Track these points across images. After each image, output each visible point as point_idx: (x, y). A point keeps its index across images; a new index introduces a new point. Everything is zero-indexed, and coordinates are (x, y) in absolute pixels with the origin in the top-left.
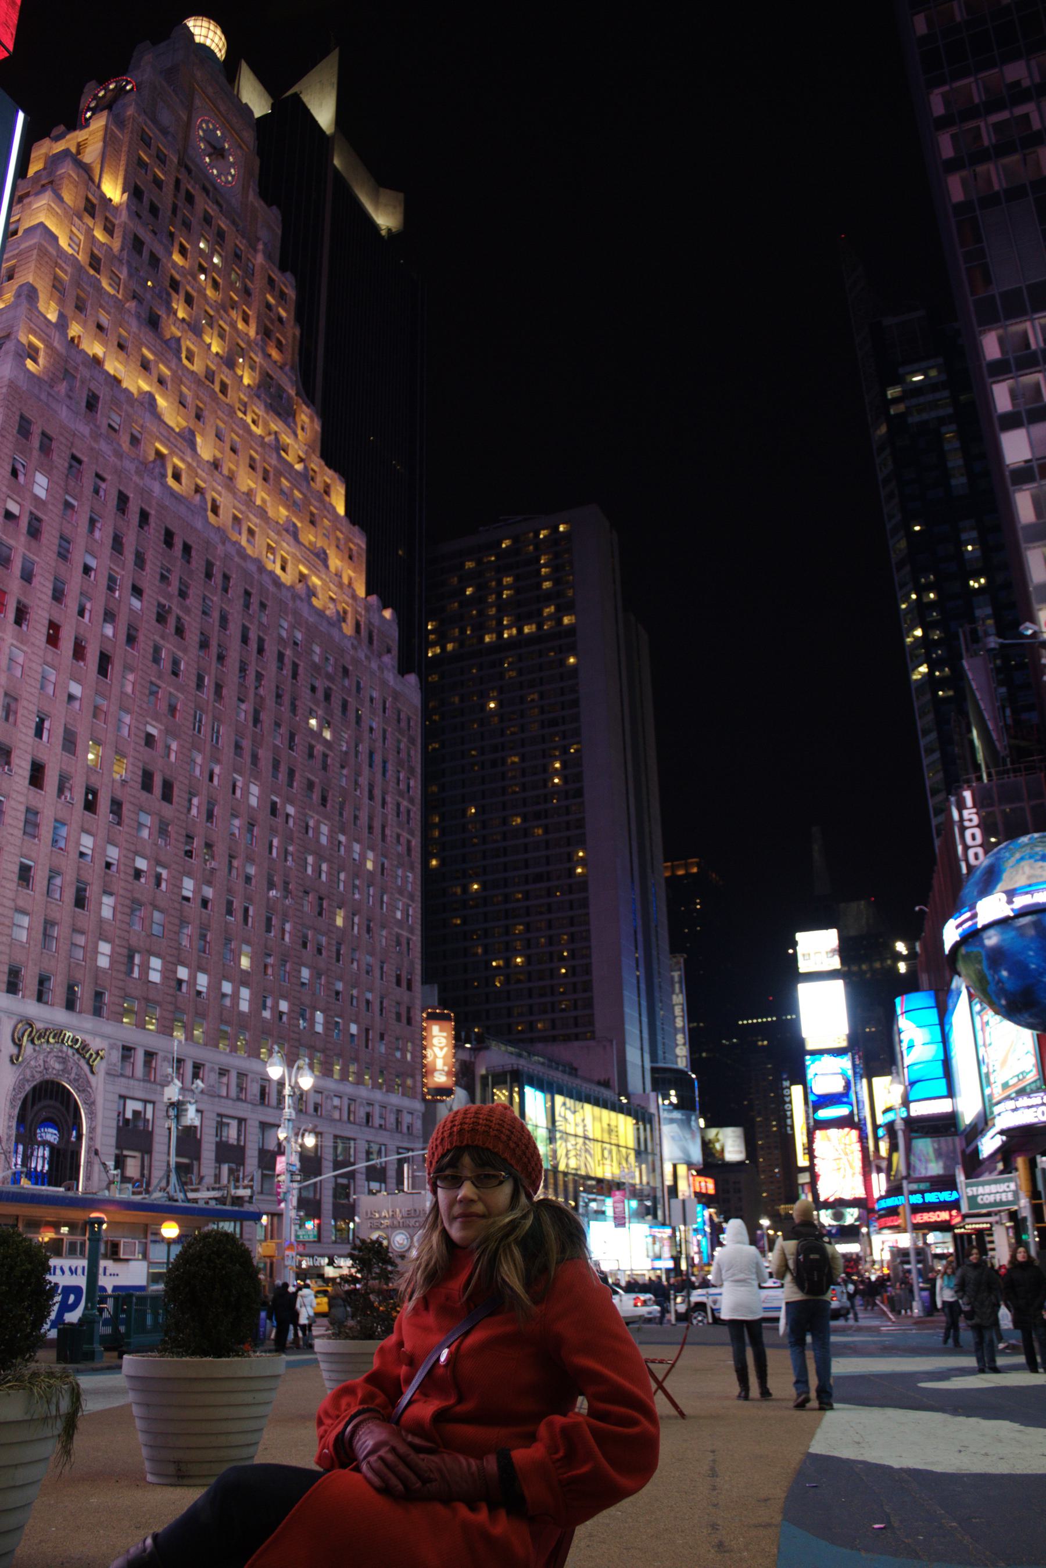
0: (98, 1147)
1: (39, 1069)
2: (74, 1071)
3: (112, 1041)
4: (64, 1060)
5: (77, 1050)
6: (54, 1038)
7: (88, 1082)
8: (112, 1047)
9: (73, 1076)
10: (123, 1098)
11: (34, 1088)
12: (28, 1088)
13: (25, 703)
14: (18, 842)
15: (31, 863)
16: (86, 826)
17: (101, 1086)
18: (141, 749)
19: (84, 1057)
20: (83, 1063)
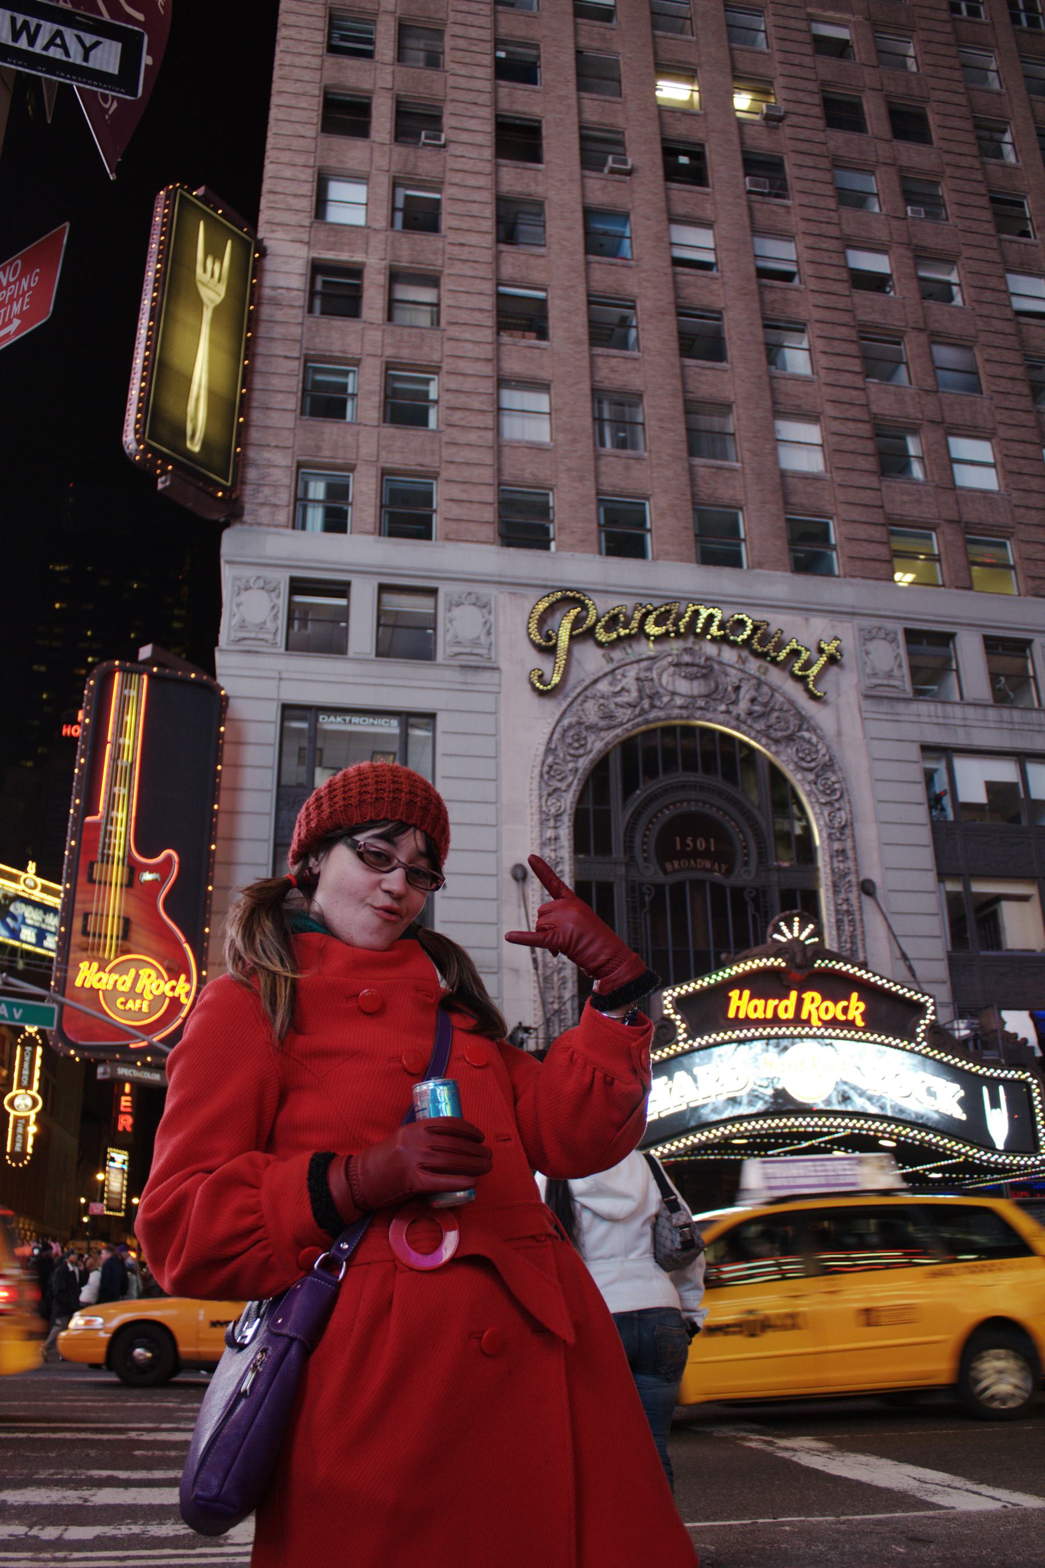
0: (873, 872)
1: (624, 698)
2: (746, 693)
3: (866, 622)
4: (706, 671)
5: (747, 643)
6: (657, 623)
7: (803, 720)
8: (868, 636)
9: (743, 706)
10: (945, 752)
11: (628, 746)
12: (596, 744)
13: (451, 30)
14: (487, 256)
15: (541, 294)
16: (680, 209)
17: (853, 729)
18: (807, 61)
19: (774, 661)
20: (776, 676)
